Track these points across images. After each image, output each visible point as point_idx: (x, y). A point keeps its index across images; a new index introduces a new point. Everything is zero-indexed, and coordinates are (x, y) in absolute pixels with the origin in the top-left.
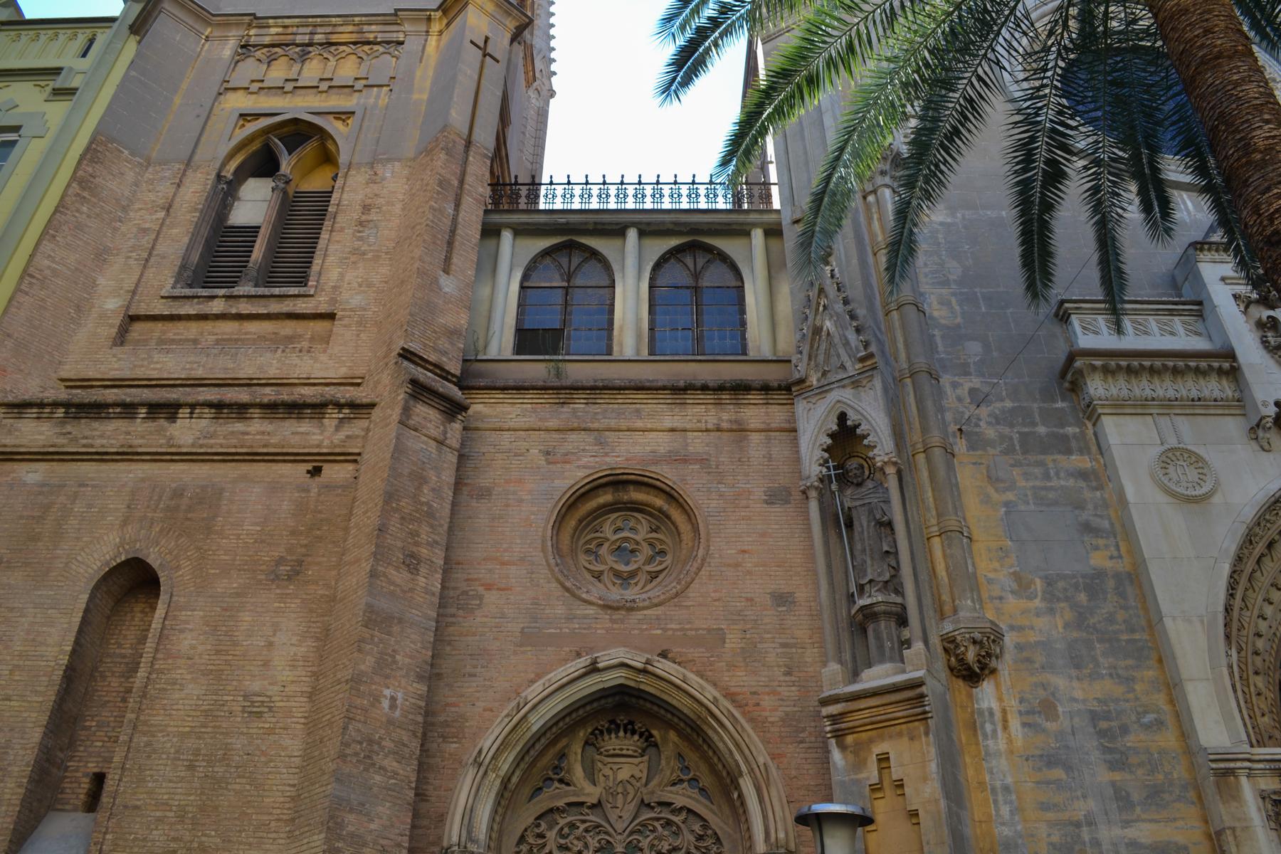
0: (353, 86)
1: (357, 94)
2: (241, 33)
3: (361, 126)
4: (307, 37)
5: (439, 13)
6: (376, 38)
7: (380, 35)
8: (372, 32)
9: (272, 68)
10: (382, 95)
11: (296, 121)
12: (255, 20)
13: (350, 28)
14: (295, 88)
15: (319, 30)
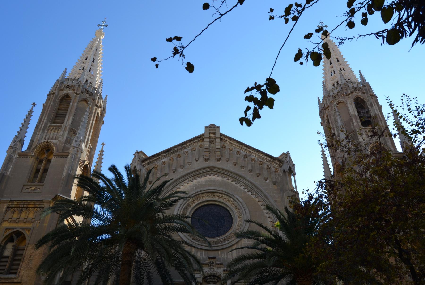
0: (31, 221)
1: (32, 223)
2: (7, 204)
3: (32, 232)
4: (23, 205)
5: (52, 201)
6: (38, 206)
7: (39, 205)
8: (38, 204)
9: (14, 214)
10: (38, 223)
11: (18, 231)
12: (10, 201)
13: (32, 203)
14: (19, 221)
15: (25, 204)
